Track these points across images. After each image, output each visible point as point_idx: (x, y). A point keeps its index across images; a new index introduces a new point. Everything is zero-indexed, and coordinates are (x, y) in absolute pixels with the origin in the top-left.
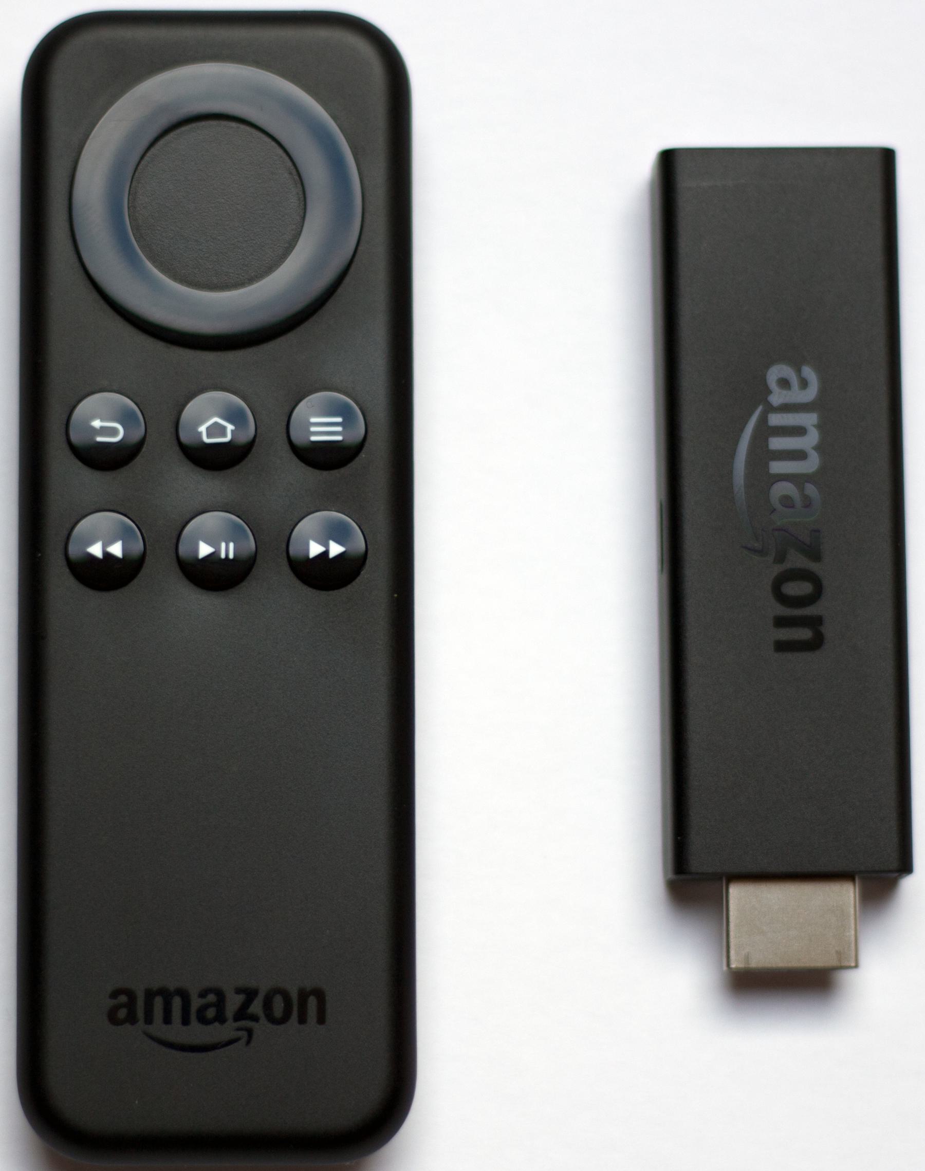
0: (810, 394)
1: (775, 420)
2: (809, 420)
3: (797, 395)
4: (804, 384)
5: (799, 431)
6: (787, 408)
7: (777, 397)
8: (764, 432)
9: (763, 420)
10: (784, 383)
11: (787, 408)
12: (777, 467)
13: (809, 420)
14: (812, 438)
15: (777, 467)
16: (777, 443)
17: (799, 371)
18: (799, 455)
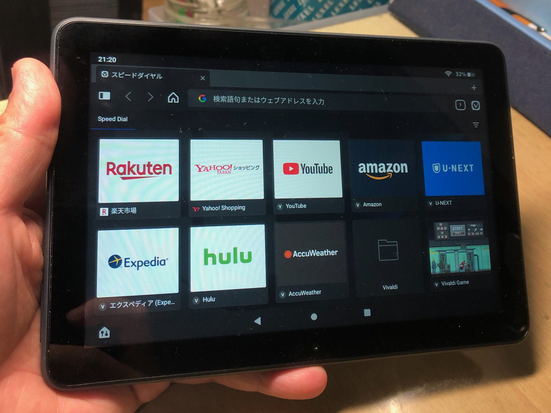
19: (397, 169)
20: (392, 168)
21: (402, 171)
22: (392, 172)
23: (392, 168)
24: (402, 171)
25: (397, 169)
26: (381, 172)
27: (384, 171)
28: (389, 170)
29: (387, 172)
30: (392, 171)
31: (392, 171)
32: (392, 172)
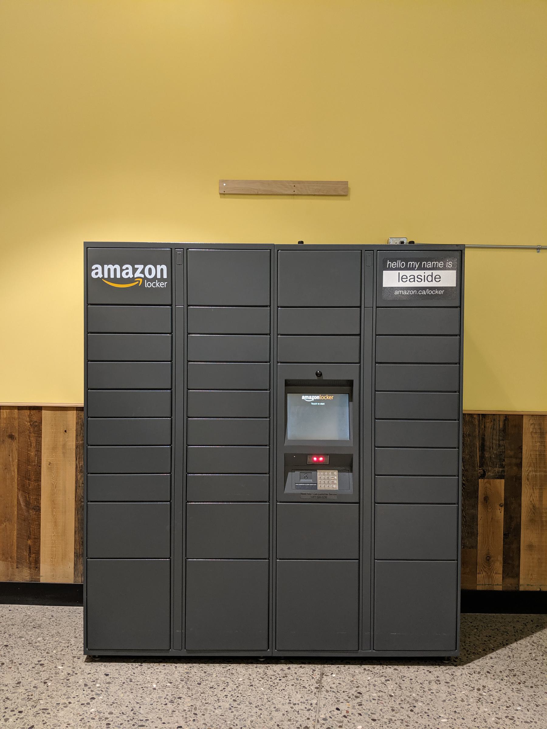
0: (100, 267)
1: (106, 276)
2: (106, 268)
3: (100, 270)
4: (97, 268)
5: (109, 270)
7: (100, 275)
8: (109, 279)
9: (105, 279)
10: (97, 274)
12: (118, 276)
13: (106, 268)
16: (112, 276)
18: (115, 270)
19: (150, 273)
20: (143, 272)
21: (159, 276)
22: (143, 277)
23: (143, 272)
24: (159, 276)
25: (150, 273)
26: (124, 276)
27: (130, 275)
28: (137, 274)
29: (135, 277)
30: (142, 276)
31: (142, 276)
32: (143, 277)
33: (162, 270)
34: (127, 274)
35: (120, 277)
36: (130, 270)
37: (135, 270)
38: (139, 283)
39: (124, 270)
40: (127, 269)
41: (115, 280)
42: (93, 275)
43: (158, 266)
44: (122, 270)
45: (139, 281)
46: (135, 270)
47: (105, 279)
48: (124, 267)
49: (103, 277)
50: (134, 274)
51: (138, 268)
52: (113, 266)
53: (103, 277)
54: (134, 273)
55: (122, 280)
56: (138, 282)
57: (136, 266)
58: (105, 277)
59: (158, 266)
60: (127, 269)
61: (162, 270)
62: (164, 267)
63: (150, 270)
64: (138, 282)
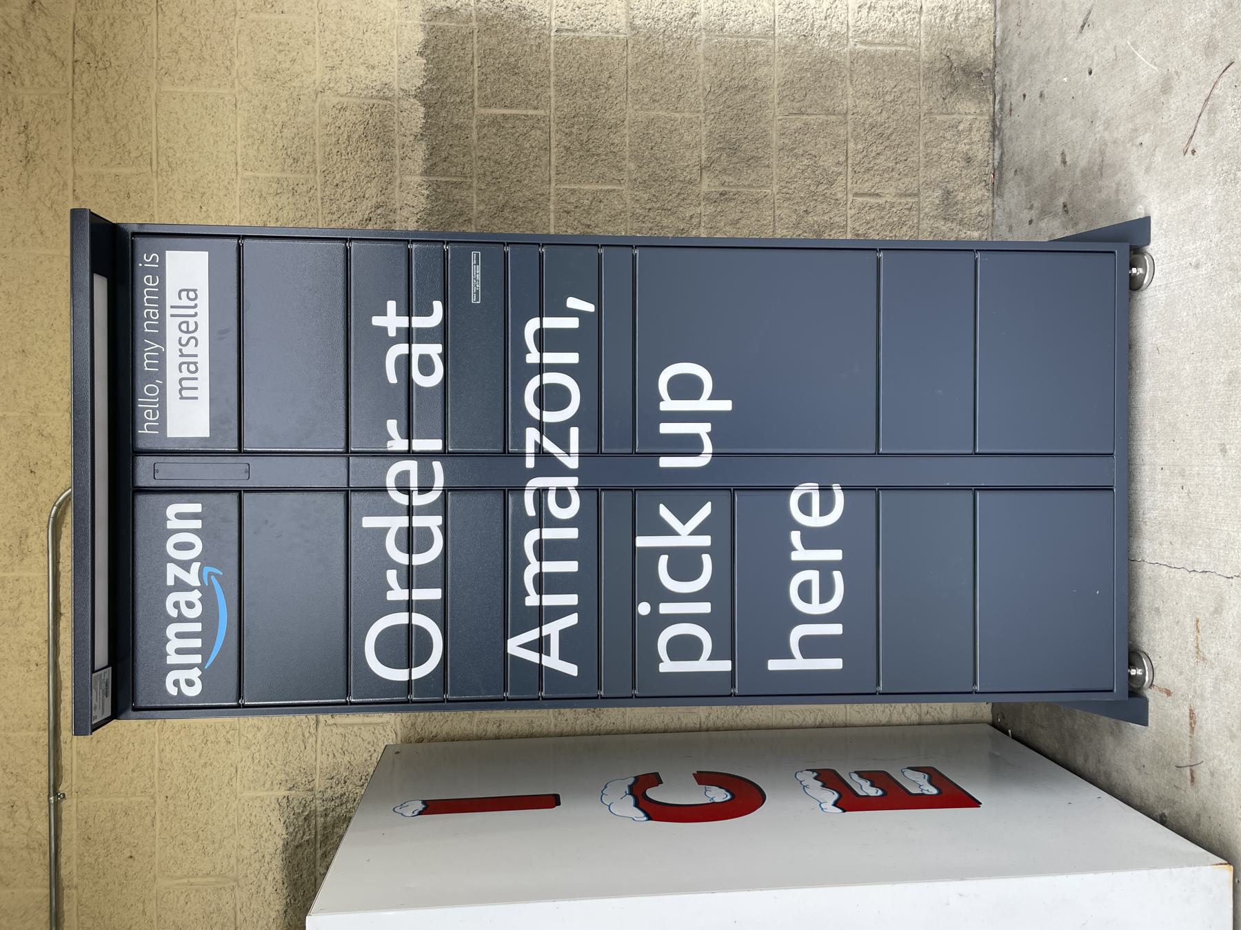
1: (197, 659)
3: (182, 675)
4: (176, 683)
5: (179, 651)
6: (189, 667)
7: (195, 674)
8: (204, 651)
10: (190, 683)
11: (189, 667)
12: (197, 627)
13: (172, 659)
14: (170, 648)
15: (197, 627)
16: (197, 643)
17: (179, 691)
18: (180, 635)
19: (188, 546)
20: (186, 565)
23: (186, 565)
25: (188, 546)
26: (197, 611)
27: (195, 596)
28: (192, 578)
30: (196, 566)
31: (196, 566)
33: (180, 516)
34: (190, 605)
35: (199, 625)
36: (182, 597)
37: (181, 586)
38: (217, 576)
39: (180, 613)
40: (176, 605)
41: (207, 635)
42: (194, 691)
43: (170, 525)
44: (181, 619)
45: (210, 574)
46: (181, 586)
47: (205, 660)
48: (173, 613)
49: (200, 666)
50: (188, 588)
51: (175, 576)
52: (168, 640)
53: (200, 666)
54: (188, 588)
55: (209, 618)
56: (213, 578)
57: (170, 582)
58: (200, 662)
59: (170, 525)
60: (176, 605)
61: (180, 516)
62: (172, 510)
63: (180, 546)
64: (213, 578)
